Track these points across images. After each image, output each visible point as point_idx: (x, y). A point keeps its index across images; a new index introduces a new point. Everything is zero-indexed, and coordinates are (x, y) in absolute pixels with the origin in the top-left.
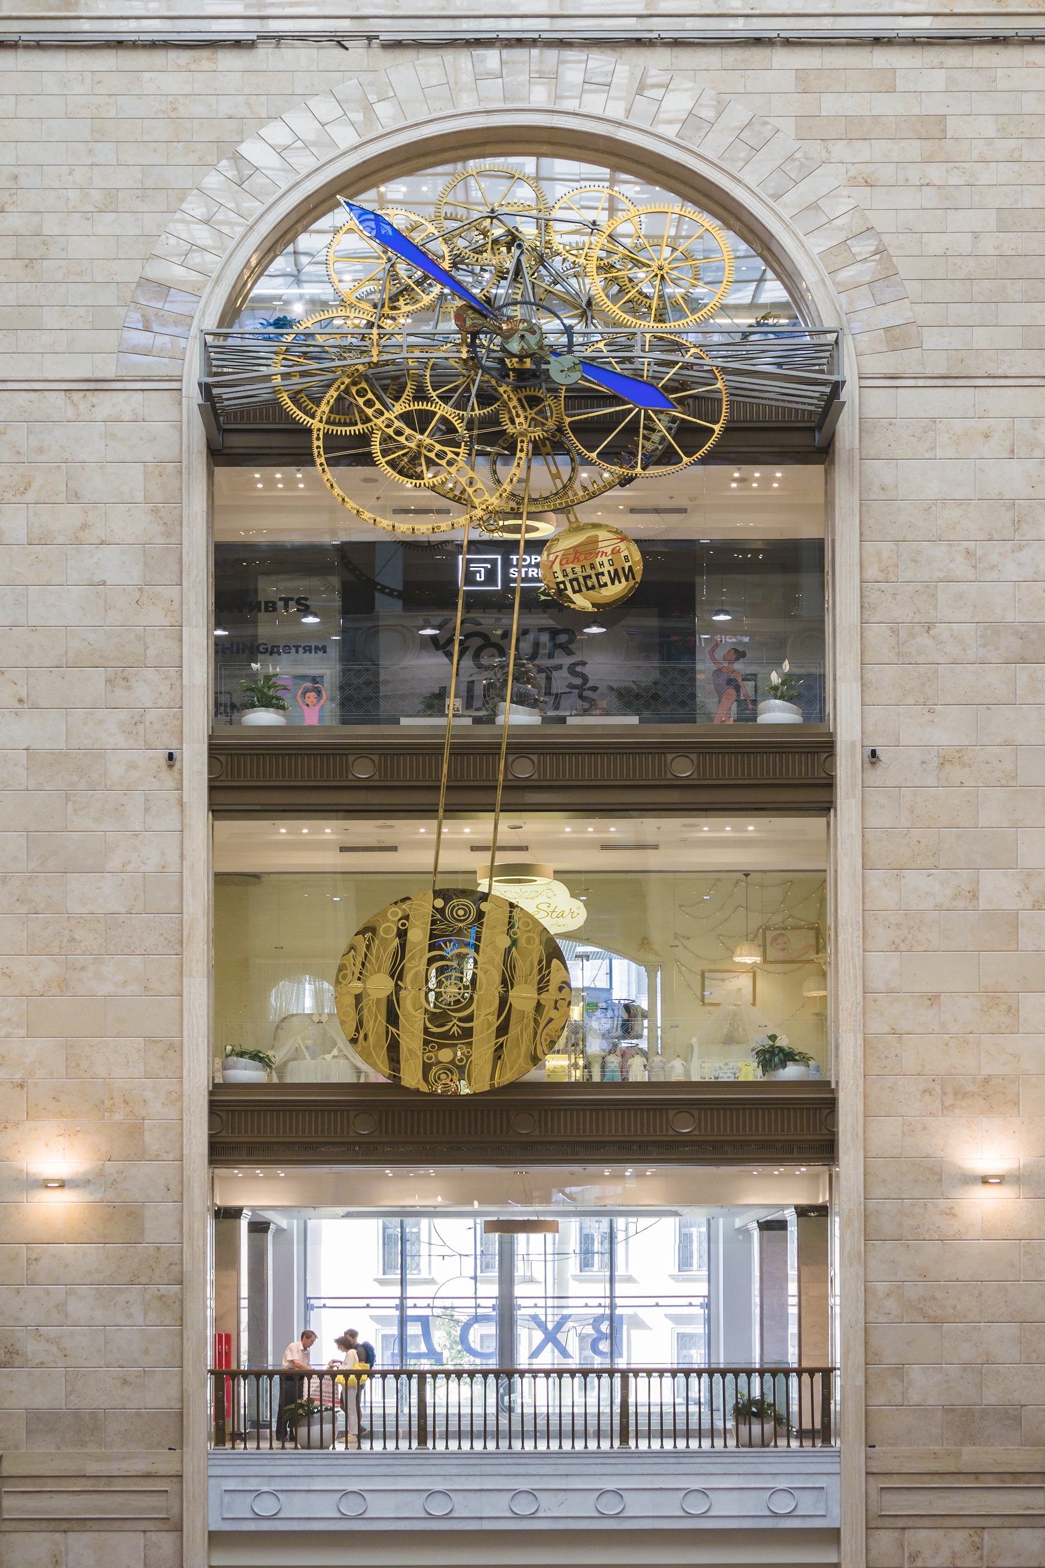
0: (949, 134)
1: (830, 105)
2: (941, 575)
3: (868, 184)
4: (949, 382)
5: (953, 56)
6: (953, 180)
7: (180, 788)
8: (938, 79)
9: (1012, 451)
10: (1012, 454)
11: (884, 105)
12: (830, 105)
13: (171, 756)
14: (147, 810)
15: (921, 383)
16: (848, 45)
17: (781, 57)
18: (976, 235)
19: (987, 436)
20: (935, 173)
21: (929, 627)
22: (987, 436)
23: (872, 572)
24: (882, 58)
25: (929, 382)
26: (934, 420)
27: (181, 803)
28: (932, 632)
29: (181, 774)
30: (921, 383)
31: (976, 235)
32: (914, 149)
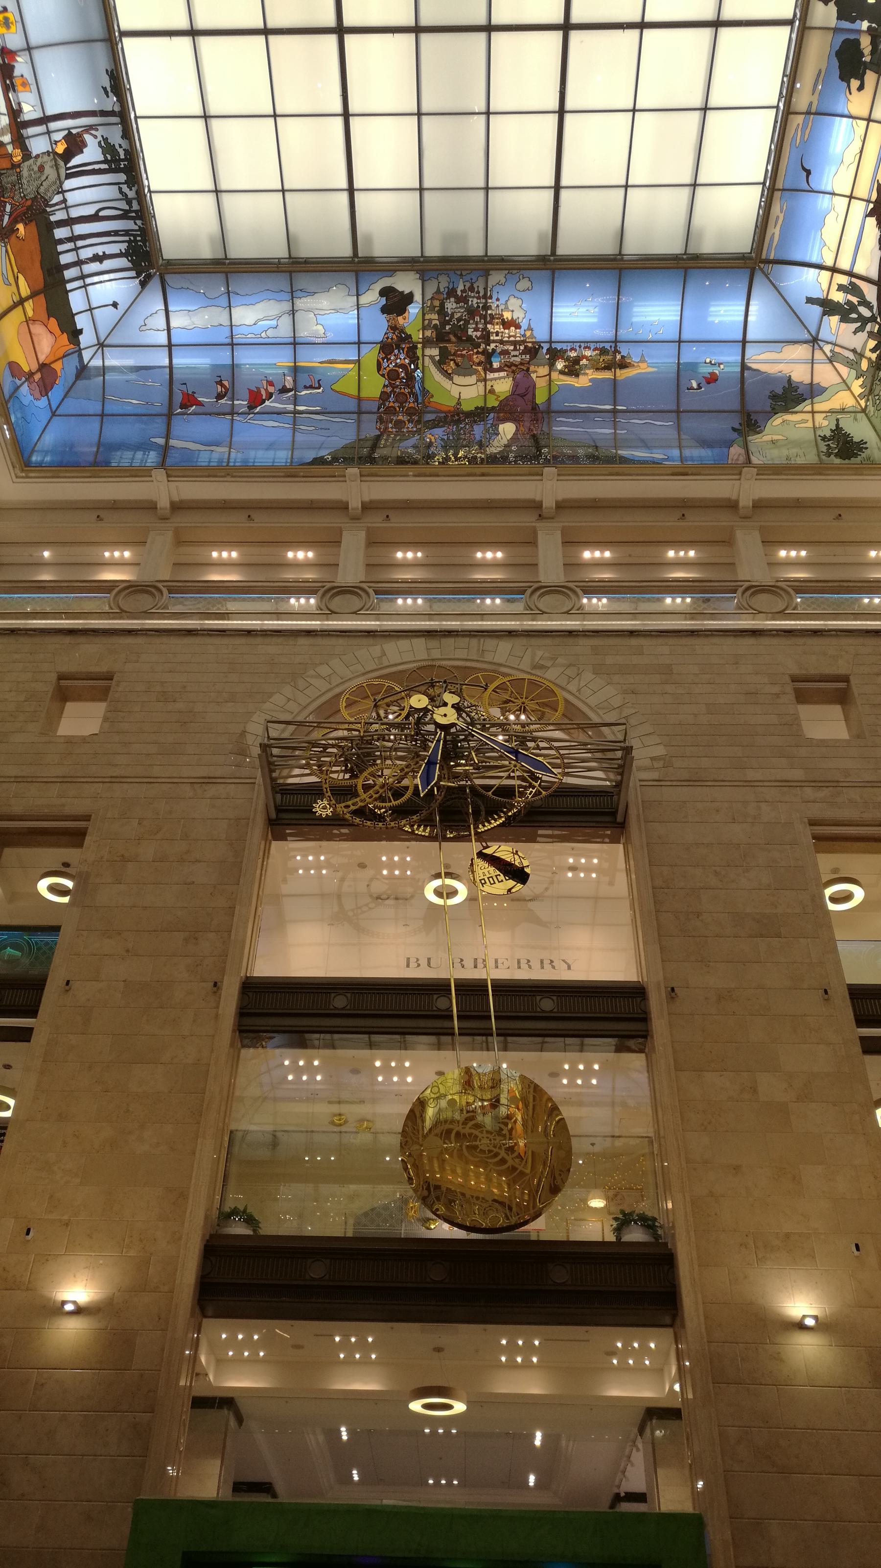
0: (674, 672)
1: (609, 660)
3: (633, 693)
4: (691, 783)
7: (217, 1007)
9: (734, 819)
10: (734, 821)
12: (609, 660)
13: (215, 984)
15: (674, 783)
17: (582, 641)
21: (698, 914)
24: (634, 641)
25: (679, 783)
26: (684, 802)
27: (217, 1016)
28: (700, 918)
29: (220, 998)
30: (674, 783)
31: (695, 715)
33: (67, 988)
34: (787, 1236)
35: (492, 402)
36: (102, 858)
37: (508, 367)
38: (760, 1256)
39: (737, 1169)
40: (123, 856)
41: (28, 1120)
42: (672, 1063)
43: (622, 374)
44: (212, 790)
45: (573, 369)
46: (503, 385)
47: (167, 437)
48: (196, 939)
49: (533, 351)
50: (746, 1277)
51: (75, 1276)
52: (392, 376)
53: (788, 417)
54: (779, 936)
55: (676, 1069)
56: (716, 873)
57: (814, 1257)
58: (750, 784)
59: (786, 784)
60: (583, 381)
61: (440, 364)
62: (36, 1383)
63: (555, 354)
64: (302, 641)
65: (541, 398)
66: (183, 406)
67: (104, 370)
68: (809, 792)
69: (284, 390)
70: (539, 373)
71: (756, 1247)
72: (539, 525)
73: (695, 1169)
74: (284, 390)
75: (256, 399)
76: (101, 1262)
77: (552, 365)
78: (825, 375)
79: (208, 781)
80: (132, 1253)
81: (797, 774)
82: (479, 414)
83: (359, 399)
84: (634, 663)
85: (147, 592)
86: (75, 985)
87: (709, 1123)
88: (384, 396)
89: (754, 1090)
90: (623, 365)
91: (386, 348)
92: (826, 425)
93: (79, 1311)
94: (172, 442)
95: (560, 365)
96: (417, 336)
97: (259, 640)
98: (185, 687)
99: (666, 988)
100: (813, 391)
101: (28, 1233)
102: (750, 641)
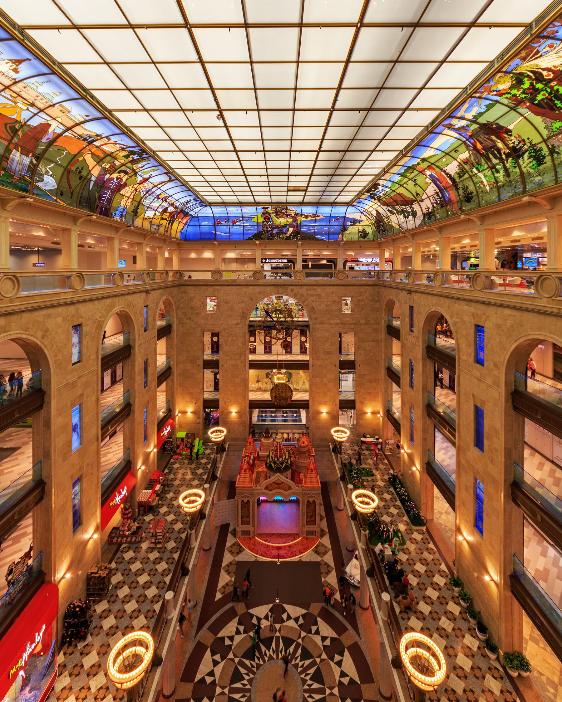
1: (310, 292)
5: (321, 287)
8: (319, 290)
11: (314, 293)
12: (310, 292)
20: (319, 300)
24: (314, 287)
32: (317, 297)
35: (288, 223)
37: (292, 217)
43: (317, 218)
44: (239, 326)
45: (306, 217)
46: (290, 220)
47: (215, 231)
49: (297, 214)
52: (265, 218)
53: (353, 227)
58: (331, 324)
59: (337, 324)
60: (308, 219)
61: (276, 216)
63: (302, 215)
64: (251, 287)
65: (299, 223)
66: (218, 224)
67: (198, 217)
68: (340, 326)
69: (240, 221)
70: (298, 218)
72: (297, 249)
74: (240, 221)
75: (234, 223)
77: (301, 216)
78: (363, 218)
79: (238, 324)
81: (339, 321)
82: (285, 226)
83: (258, 223)
88: (263, 222)
90: (318, 217)
91: (263, 214)
92: (361, 229)
94: (217, 233)
95: (303, 216)
96: (270, 212)
100: (360, 221)
102: (336, 287)
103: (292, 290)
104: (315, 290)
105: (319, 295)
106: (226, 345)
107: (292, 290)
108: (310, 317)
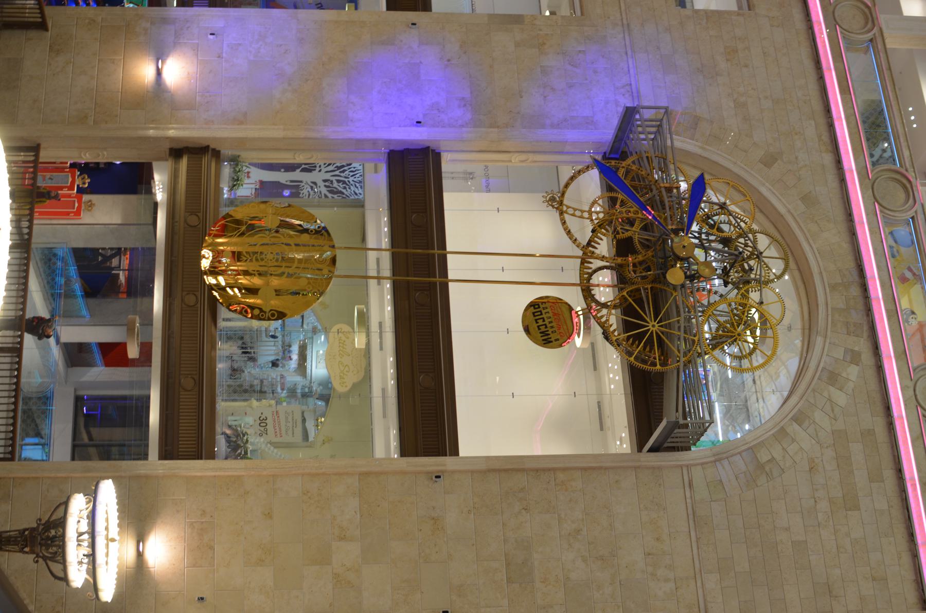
0: (849, 513)
1: (856, 449)
2: (563, 516)
3: (811, 469)
4: (691, 517)
6: (820, 516)
9: (649, 554)
12: (856, 449)
14: (387, 114)
16: (894, 456)
18: (787, 529)
19: (658, 539)
20: (823, 505)
22: (658, 539)
23: (561, 476)
24: (889, 474)
28: (523, 511)
30: (689, 501)
33: (410, 25)
34: (212, 548)
36: (540, 30)
38: (194, 524)
39: (269, 515)
40: (544, 44)
41: (298, 20)
42: (364, 469)
48: (465, 105)
50: (178, 511)
51: (183, 67)
54: (509, 581)
55: (361, 474)
56: (578, 531)
57: (194, 566)
62: (114, 59)
71: (202, 523)
73: (268, 482)
76: (192, 81)
80: (198, 99)
84: (855, 472)
85: (867, 23)
86: (414, 31)
87: (310, 498)
89: (342, 538)
93: (159, 73)
97: (822, 121)
98: (746, 66)
99: (443, 472)
101: (211, 34)
103: (854, 357)
104: (875, 477)
105: (851, 503)
106: (517, 45)
107: (854, 357)
108: (722, 454)
